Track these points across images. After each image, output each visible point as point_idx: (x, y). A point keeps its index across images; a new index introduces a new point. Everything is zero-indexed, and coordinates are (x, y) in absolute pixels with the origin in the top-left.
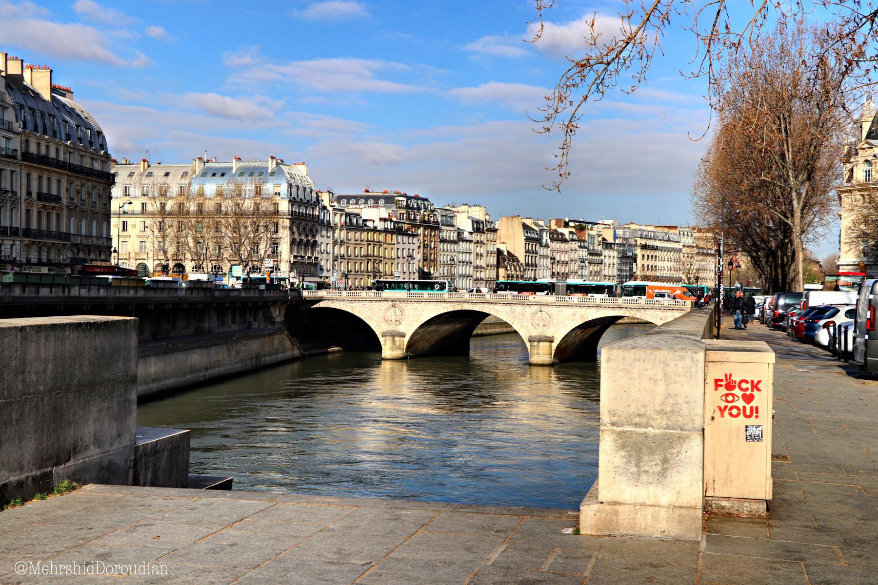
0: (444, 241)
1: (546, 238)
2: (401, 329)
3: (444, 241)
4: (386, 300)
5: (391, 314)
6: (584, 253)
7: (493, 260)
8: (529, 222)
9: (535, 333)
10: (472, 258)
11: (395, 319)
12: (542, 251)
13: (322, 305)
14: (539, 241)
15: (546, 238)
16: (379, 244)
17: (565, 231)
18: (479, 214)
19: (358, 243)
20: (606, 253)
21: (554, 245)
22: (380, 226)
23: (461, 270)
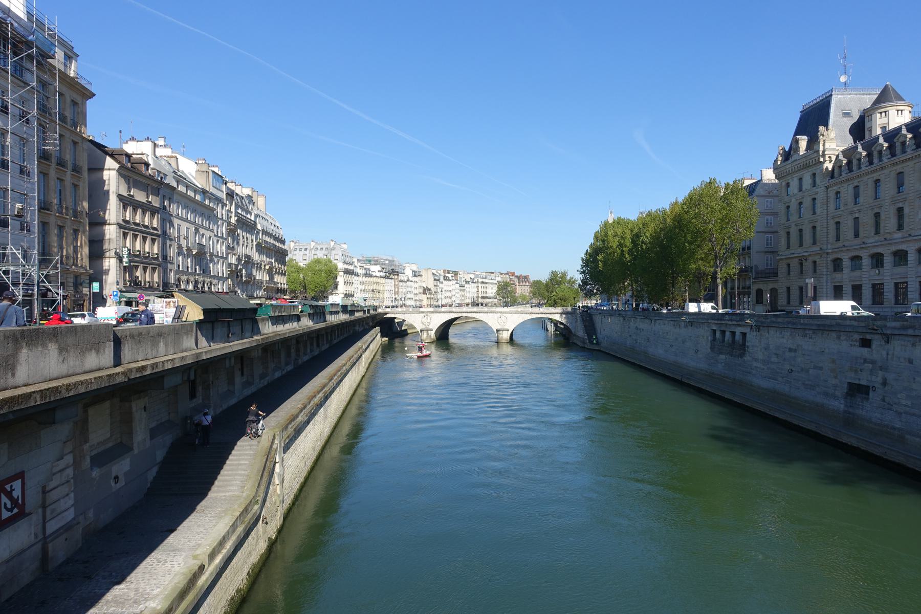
0: (401, 281)
1: (442, 279)
2: (430, 327)
3: (401, 281)
4: (422, 312)
5: (425, 320)
6: (458, 286)
7: (421, 291)
8: (434, 271)
9: (499, 327)
10: (413, 289)
11: (424, 323)
12: (441, 286)
13: (388, 316)
14: (438, 280)
15: (442, 279)
16: (378, 283)
17: (450, 275)
18: (415, 268)
19: (370, 283)
20: (467, 286)
21: (445, 282)
22: (378, 274)
23: (408, 296)
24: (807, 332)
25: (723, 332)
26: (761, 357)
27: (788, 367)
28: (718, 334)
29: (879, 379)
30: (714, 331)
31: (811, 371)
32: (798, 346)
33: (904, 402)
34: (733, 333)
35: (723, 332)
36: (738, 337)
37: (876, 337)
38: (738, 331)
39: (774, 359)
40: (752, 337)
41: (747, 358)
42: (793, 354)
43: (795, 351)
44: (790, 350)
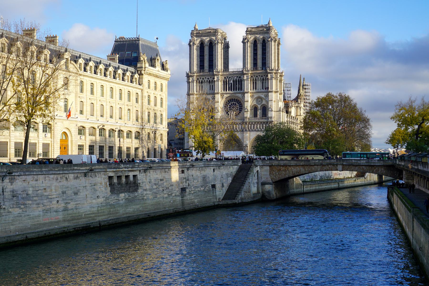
24: (166, 170)
25: (119, 177)
26: (148, 187)
27: (161, 189)
28: (115, 180)
29: (187, 184)
30: (110, 178)
31: (170, 188)
32: (164, 177)
33: (193, 189)
34: (127, 177)
35: (119, 177)
36: (131, 178)
37: (185, 169)
38: (131, 174)
39: (155, 187)
40: (141, 177)
41: (140, 191)
42: (162, 182)
43: (163, 180)
44: (161, 180)
